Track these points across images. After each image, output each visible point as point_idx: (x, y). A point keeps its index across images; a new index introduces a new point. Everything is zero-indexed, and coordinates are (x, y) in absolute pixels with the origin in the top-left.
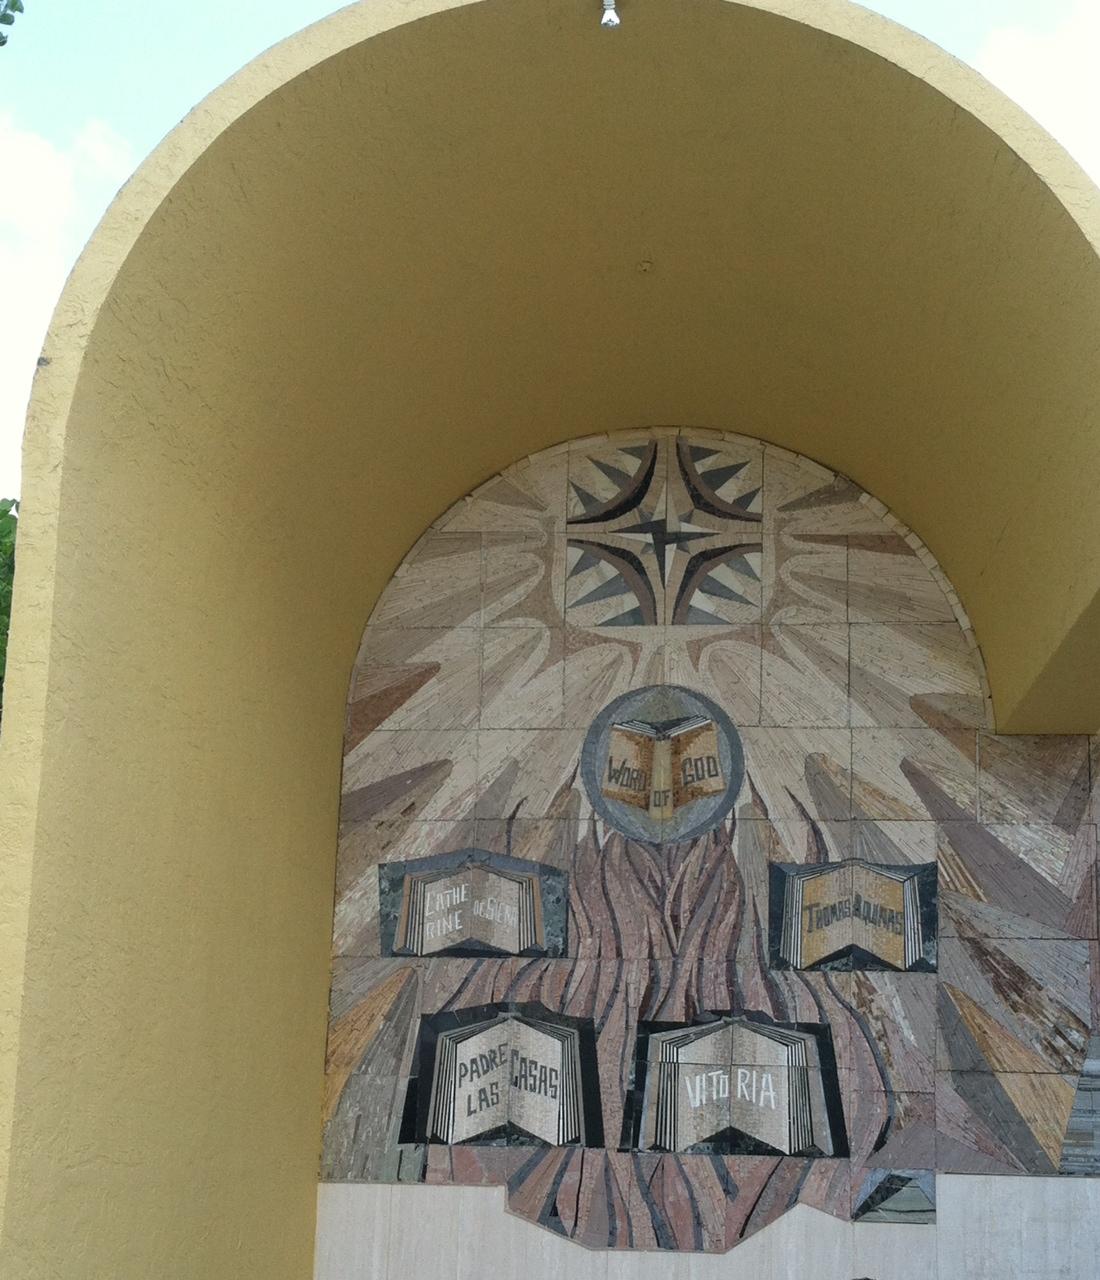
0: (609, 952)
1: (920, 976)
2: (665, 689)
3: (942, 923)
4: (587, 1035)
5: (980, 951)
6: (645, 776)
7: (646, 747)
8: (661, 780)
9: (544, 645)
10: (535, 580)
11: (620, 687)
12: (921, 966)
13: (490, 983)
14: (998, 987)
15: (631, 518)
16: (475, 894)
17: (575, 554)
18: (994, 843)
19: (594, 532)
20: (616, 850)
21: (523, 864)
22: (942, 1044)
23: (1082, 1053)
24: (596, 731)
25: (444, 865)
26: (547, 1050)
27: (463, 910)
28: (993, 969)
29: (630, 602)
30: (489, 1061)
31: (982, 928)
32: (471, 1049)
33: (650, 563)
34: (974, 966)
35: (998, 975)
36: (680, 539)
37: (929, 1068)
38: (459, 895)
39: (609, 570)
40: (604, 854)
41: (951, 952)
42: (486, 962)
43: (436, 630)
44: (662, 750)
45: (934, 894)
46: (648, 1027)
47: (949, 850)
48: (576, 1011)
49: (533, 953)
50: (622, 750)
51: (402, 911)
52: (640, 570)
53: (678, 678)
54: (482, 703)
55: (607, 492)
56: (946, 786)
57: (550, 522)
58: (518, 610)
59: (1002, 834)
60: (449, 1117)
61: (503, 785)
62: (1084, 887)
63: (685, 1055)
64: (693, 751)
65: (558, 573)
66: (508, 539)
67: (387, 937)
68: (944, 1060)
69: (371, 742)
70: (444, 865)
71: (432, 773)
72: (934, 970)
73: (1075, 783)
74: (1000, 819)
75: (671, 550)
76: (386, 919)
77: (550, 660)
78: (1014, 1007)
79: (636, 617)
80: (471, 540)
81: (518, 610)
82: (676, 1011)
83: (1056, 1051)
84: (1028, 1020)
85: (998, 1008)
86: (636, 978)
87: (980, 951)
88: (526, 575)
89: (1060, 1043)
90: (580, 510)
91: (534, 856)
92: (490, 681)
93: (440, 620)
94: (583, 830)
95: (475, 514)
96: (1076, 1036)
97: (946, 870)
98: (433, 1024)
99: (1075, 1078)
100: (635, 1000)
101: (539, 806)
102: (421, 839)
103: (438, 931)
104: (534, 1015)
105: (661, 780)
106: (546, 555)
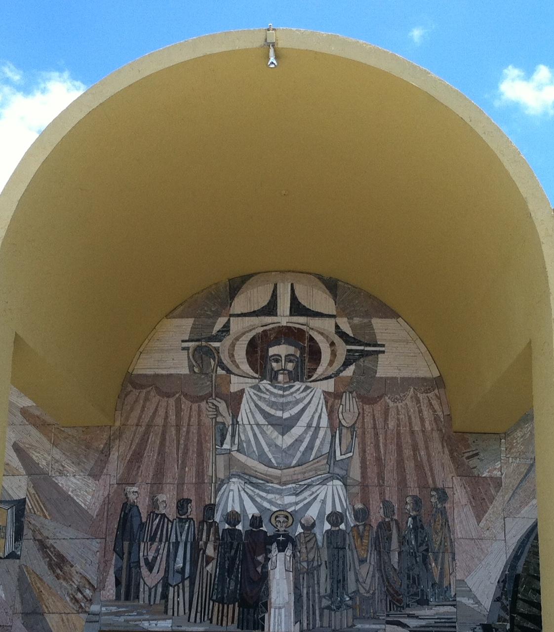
1: (10, 561)
3: (25, 532)
5: (43, 546)
12: (13, 556)
14: (50, 566)
18: (56, 486)
22: (18, 599)
23: (90, 601)
28: (49, 556)
31: (45, 534)
34: (39, 555)
35: (51, 559)
37: (10, 612)
41: (28, 546)
45: (23, 515)
47: (32, 491)
56: (35, 456)
59: (61, 481)
62: (100, 510)
68: (19, 607)
72: (18, 557)
73: (102, 452)
74: (61, 473)
78: (58, 577)
83: (77, 601)
84: (64, 584)
85: (49, 578)
87: (43, 546)
89: (79, 596)
96: (88, 592)
97: (30, 501)
99: (86, 615)
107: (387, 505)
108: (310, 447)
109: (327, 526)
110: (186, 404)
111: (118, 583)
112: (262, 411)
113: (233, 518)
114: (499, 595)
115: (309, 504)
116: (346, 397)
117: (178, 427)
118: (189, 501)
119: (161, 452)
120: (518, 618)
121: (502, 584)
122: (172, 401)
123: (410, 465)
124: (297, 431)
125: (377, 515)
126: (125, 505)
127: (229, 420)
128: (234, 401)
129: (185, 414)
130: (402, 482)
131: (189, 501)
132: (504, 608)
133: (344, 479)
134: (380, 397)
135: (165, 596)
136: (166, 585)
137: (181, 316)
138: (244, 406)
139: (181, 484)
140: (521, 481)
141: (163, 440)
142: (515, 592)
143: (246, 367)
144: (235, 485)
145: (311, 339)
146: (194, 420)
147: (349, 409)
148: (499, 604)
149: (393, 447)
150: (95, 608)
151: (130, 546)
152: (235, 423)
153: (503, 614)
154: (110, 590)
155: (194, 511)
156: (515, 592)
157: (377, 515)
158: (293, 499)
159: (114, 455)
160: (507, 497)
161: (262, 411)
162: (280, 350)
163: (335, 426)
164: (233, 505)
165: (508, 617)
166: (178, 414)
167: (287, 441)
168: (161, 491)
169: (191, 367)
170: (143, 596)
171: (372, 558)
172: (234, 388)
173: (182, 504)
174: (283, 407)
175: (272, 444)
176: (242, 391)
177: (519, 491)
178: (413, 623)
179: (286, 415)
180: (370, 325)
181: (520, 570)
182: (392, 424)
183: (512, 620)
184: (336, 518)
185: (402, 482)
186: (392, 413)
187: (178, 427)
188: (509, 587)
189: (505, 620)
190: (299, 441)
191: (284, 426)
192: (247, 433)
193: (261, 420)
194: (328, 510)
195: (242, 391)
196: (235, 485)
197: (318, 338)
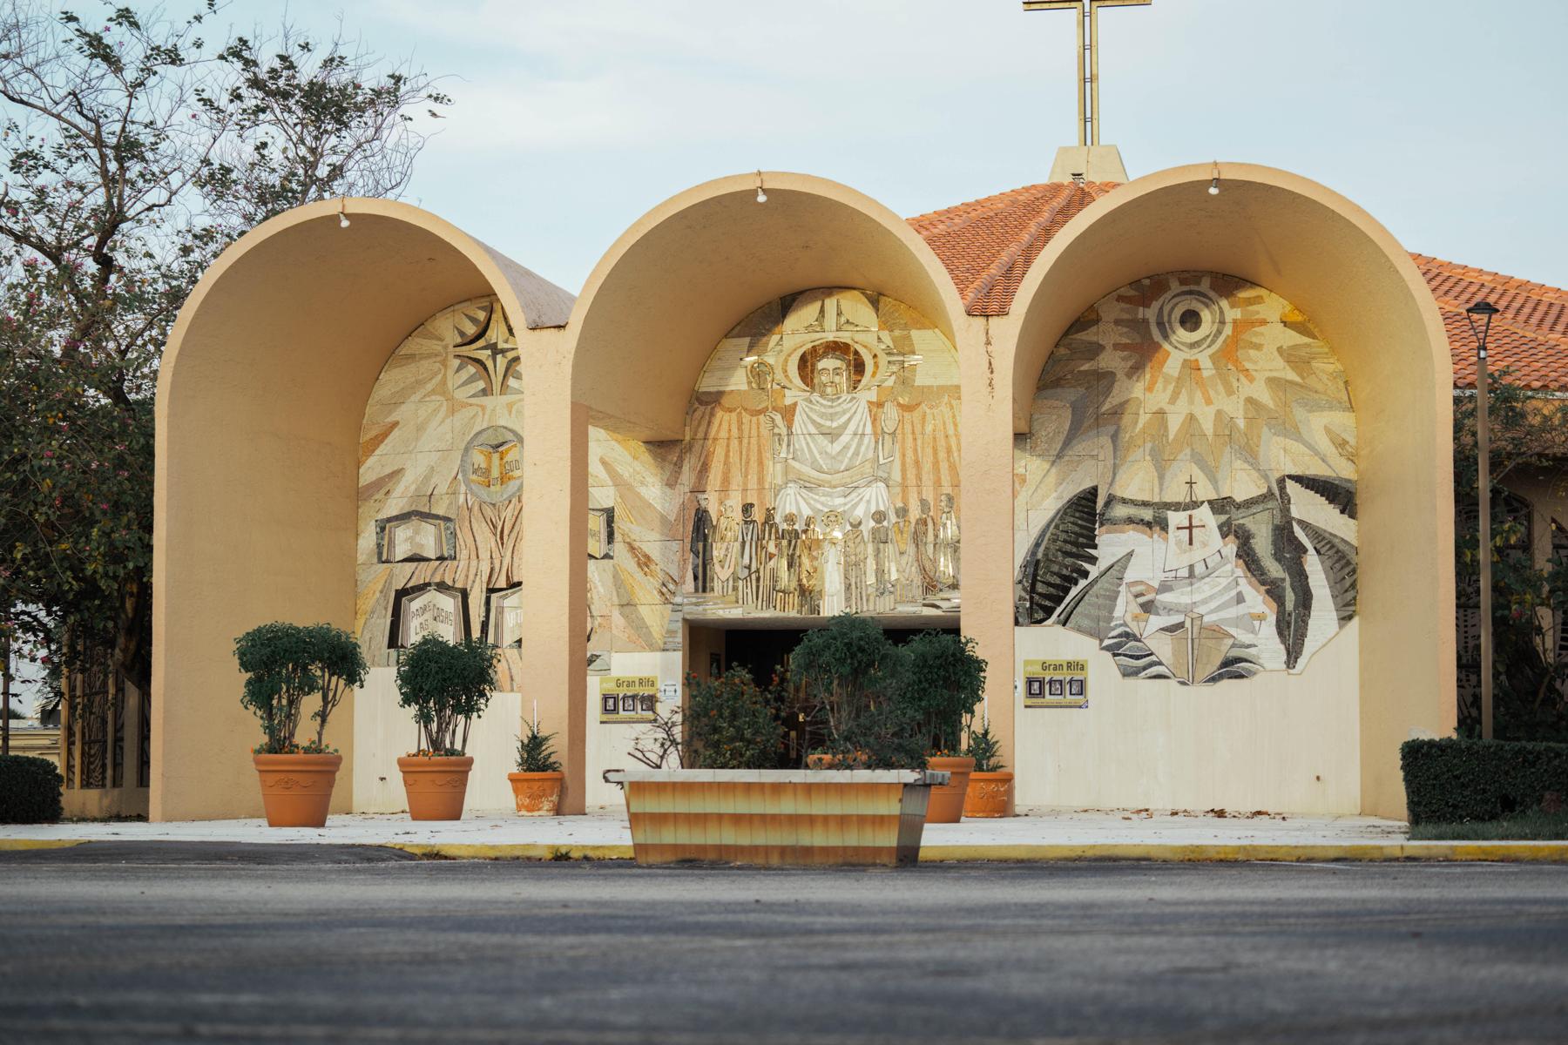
0: (473, 556)
1: (606, 561)
2: (495, 428)
3: (616, 535)
4: (465, 594)
5: (632, 548)
6: (488, 471)
7: (489, 458)
8: (495, 473)
9: (444, 409)
10: (440, 376)
11: (477, 429)
12: (607, 556)
13: (423, 573)
14: (639, 565)
15: (481, 343)
16: (417, 532)
17: (457, 362)
18: (638, 495)
19: (465, 351)
20: (476, 508)
21: (437, 517)
22: (615, 593)
24: (467, 450)
25: (403, 517)
26: (449, 604)
27: (411, 539)
28: (637, 556)
29: (481, 385)
30: (424, 609)
31: (633, 537)
32: (416, 604)
33: (490, 364)
34: (629, 555)
35: (639, 559)
36: (503, 351)
37: (609, 604)
38: (409, 533)
39: (472, 369)
40: (470, 510)
41: (619, 548)
42: (422, 563)
43: (397, 404)
44: (496, 457)
45: (613, 522)
46: (491, 591)
47: (620, 500)
48: (459, 585)
49: (441, 558)
50: (478, 458)
51: (385, 542)
52: (486, 369)
53: (502, 422)
54: (417, 439)
55: (471, 330)
56: (619, 469)
57: (446, 347)
58: (433, 392)
59: (643, 491)
60: (408, 635)
61: (427, 478)
62: (677, 516)
63: (507, 603)
64: (508, 458)
65: (450, 372)
66: (429, 356)
67: (380, 554)
68: (616, 600)
69: (371, 461)
70: (403, 517)
71: (396, 474)
72: (612, 558)
73: (675, 464)
74: (642, 483)
75: (499, 357)
76: (379, 546)
77: (447, 417)
78: (645, 574)
79: (484, 392)
80: (411, 357)
81: (433, 392)
82: (502, 583)
83: (663, 594)
84: (651, 580)
85: (639, 575)
86: (485, 568)
87: (632, 548)
88: (436, 374)
89: (664, 590)
90: (459, 340)
91: (441, 512)
92: (420, 428)
93: (396, 402)
94: (462, 499)
95: (411, 346)
96: (671, 587)
98: (402, 594)
99: (670, 606)
100: (485, 578)
101: (443, 488)
102: (393, 508)
103: (401, 551)
104: (442, 587)
105: (495, 473)
106: (444, 363)
107: (924, 503)
108: (856, 453)
109: (872, 524)
110: (746, 418)
111: (696, 578)
112: (814, 422)
113: (790, 519)
114: (1020, 578)
115: (857, 504)
116: (888, 405)
117: (740, 439)
118: (752, 505)
119: (726, 463)
120: (1036, 597)
121: (1023, 569)
122: (734, 415)
123: (944, 466)
124: (845, 439)
125: (915, 513)
126: (698, 510)
127: (784, 431)
128: (789, 413)
129: (746, 427)
130: (938, 483)
131: (752, 505)
132: (1024, 589)
133: (886, 481)
134: (918, 405)
135: (735, 589)
136: (736, 579)
137: (739, 336)
138: (797, 418)
139: (745, 490)
140: (1044, 476)
141: (728, 451)
142: (1035, 575)
143: (797, 381)
144: (792, 490)
145: (856, 353)
146: (754, 433)
147: (891, 413)
148: (1020, 586)
149: (929, 451)
150: (678, 600)
151: (705, 546)
152: (790, 434)
153: (1024, 594)
154: (690, 585)
155: (758, 515)
156: (1035, 575)
157: (915, 513)
158: (842, 500)
159: (686, 468)
160: (1030, 492)
161: (814, 422)
162: (828, 363)
163: (879, 434)
164: (790, 508)
165: (1028, 597)
166: (740, 429)
167: (837, 447)
168: (727, 497)
169: (749, 383)
170: (717, 585)
171: (911, 549)
172: (788, 401)
173: (747, 508)
174: (832, 417)
175: (824, 453)
176: (795, 404)
177: (1042, 486)
178: (944, 605)
179: (835, 425)
180: (909, 337)
181: (1040, 555)
182: (929, 428)
183: (1032, 599)
184: (879, 516)
185: (938, 483)
186: (929, 417)
187: (740, 439)
188: (1030, 570)
189: (1025, 600)
190: (846, 447)
191: (833, 435)
192: (800, 442)
193: (813, 430)
194: (873, 510)
195: (795, 404)
196: (792, 490)
197: (862, 351)
